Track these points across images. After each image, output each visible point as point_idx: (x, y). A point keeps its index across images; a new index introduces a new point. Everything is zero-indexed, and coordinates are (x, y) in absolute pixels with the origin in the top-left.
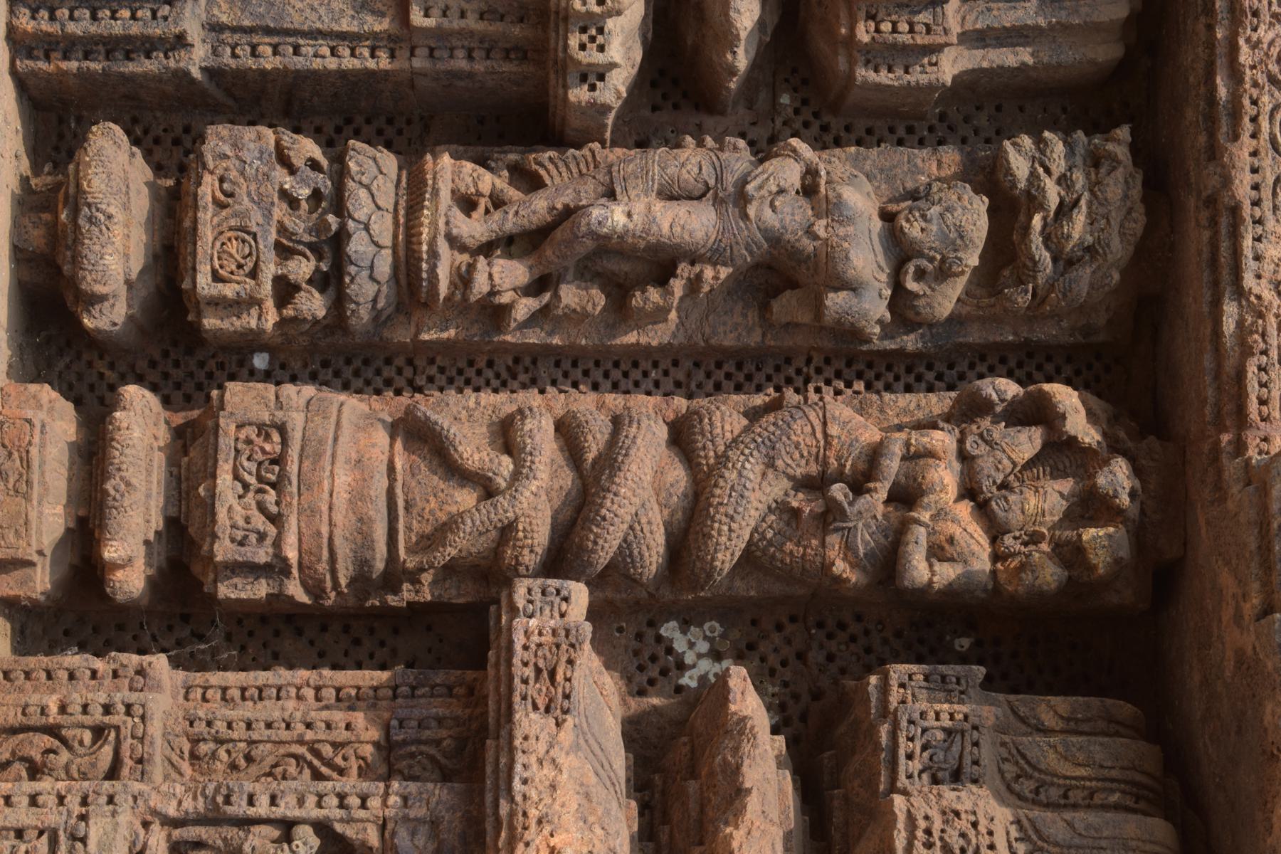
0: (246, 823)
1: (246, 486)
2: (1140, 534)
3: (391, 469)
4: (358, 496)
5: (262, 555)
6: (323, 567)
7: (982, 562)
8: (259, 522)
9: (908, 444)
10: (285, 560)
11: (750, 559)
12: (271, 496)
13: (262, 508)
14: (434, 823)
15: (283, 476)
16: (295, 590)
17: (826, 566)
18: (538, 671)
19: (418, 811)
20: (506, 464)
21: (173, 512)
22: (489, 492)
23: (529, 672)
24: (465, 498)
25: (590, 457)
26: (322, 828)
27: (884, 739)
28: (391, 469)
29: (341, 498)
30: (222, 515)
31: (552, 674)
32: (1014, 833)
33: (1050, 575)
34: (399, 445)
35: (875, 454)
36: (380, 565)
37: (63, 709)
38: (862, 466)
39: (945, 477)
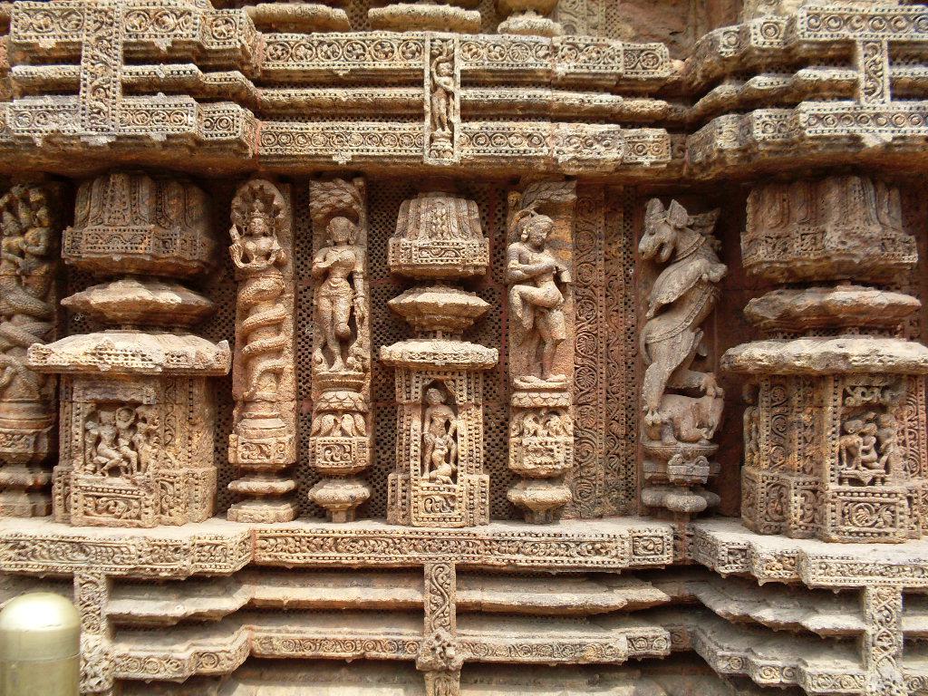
0: (85, 443)
1: (13, 444)
2: (33, 185)
3: (10, 402)
4: (17, 411)
5: (32, 439)
6: (39, 422)
7: (42, 231)
8: (23, 440)
9: (5, 252)
10: (34, 433)
11: (44, 298)
12: (16, 437)
13: (19, 439)
14: (85, 389)
15: (9, 433)
16: (46, 431)
17: (43, 276)
18: (44, 359)
19: (81, 393)
20: (9, 368)
21: (24, 465)
22: (16, 374)
23: (44, 361)
24: (18, 381)
25: (9, 344)
26: (86, 420)
27: (74, 260)
28: (10, 402)
29: (17, 416)
30: (20, 451)
31: (45, 354)
32: (95, 223)
33: (42, 212)
34: (4, 400)
35: (11, 261)
36: (39, 405)
37: (60, 494)
38: (12, 265)
39: (17, 241)
